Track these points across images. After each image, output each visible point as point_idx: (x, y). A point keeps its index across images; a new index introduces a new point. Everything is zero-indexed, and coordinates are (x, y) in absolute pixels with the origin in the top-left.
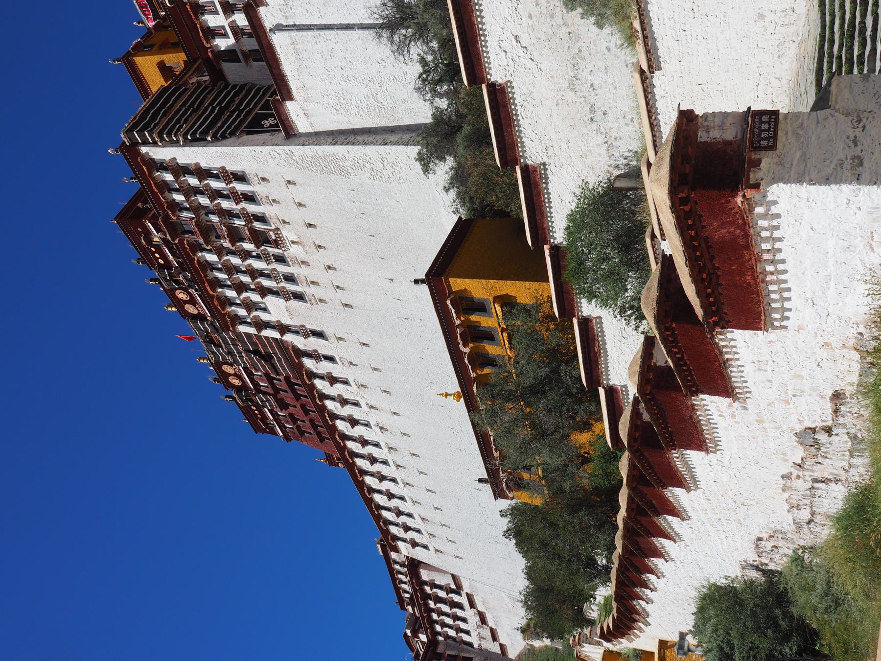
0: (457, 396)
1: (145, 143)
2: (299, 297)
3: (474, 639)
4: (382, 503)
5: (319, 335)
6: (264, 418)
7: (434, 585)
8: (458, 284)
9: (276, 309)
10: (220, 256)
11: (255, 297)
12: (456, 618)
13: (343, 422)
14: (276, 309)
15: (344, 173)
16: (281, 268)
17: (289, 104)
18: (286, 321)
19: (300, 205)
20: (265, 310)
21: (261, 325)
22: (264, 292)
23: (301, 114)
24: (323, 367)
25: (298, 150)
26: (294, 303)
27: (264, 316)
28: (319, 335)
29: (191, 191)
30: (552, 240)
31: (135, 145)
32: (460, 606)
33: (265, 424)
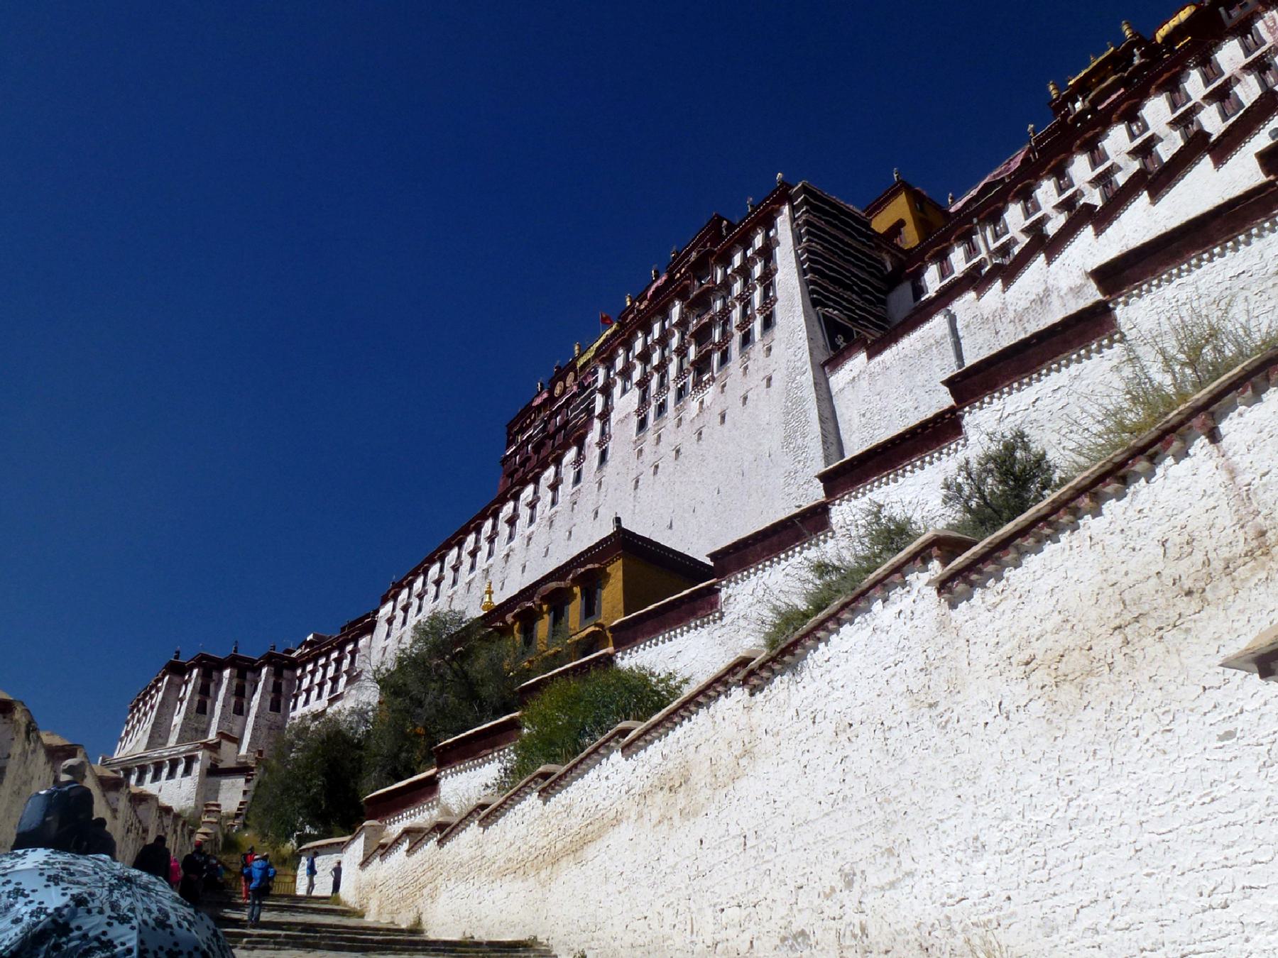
1: (794, 209)
3: (301, 710)
4: (430, 573)
5: (603, 458)
6: (523, 431)
7: (353, 653)
8: (616, 571)
9: (625, 402)
10: (678, 325)
11: (636, 375)
12: (321, 685)
13: (511, 511)
15: (788, 439)
16: (671, 396)
17: (862, 356)
18: (614, 417)
19: (745, 399)
21: (607, 391)
22: (643, 384)
23: (854, 374)
24: (568, 474)
25: (808, 378)
26: (635, 421)
27: (617, 391)
28: (603, 458)
29: (745, 271)
30: (619, 654)
31: (790, 200)
33: (517, 433)
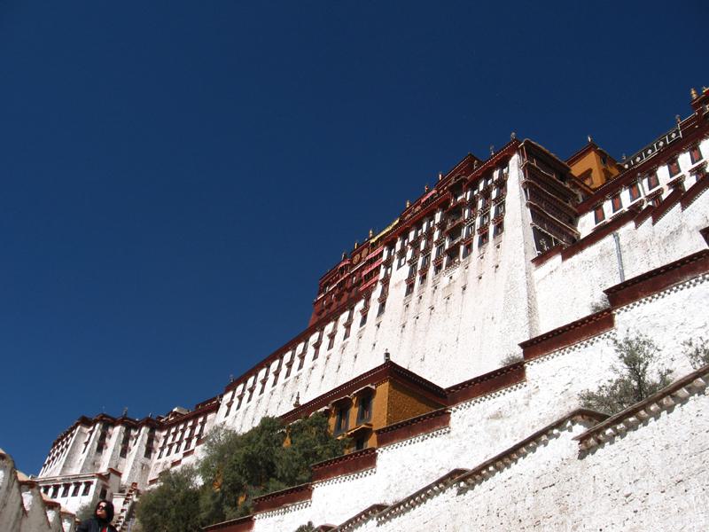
0: (297, 404)
2: (410, 287)
5: (382, 310)
7: (203, 424)
8: (383, 390)
9: (399, 274)
10: (438, 225)
12: (179, 443)
14: (399, 274)
17: (559, 258)
18: (392, 282)
20: (399, 266)
21: (388, 264)
22: (413, 263)
23: (553, 269)
24: (357, 317)
26: (404, 287)
28: (382, 310)
29: (486, 194)
32: (186, 448)
